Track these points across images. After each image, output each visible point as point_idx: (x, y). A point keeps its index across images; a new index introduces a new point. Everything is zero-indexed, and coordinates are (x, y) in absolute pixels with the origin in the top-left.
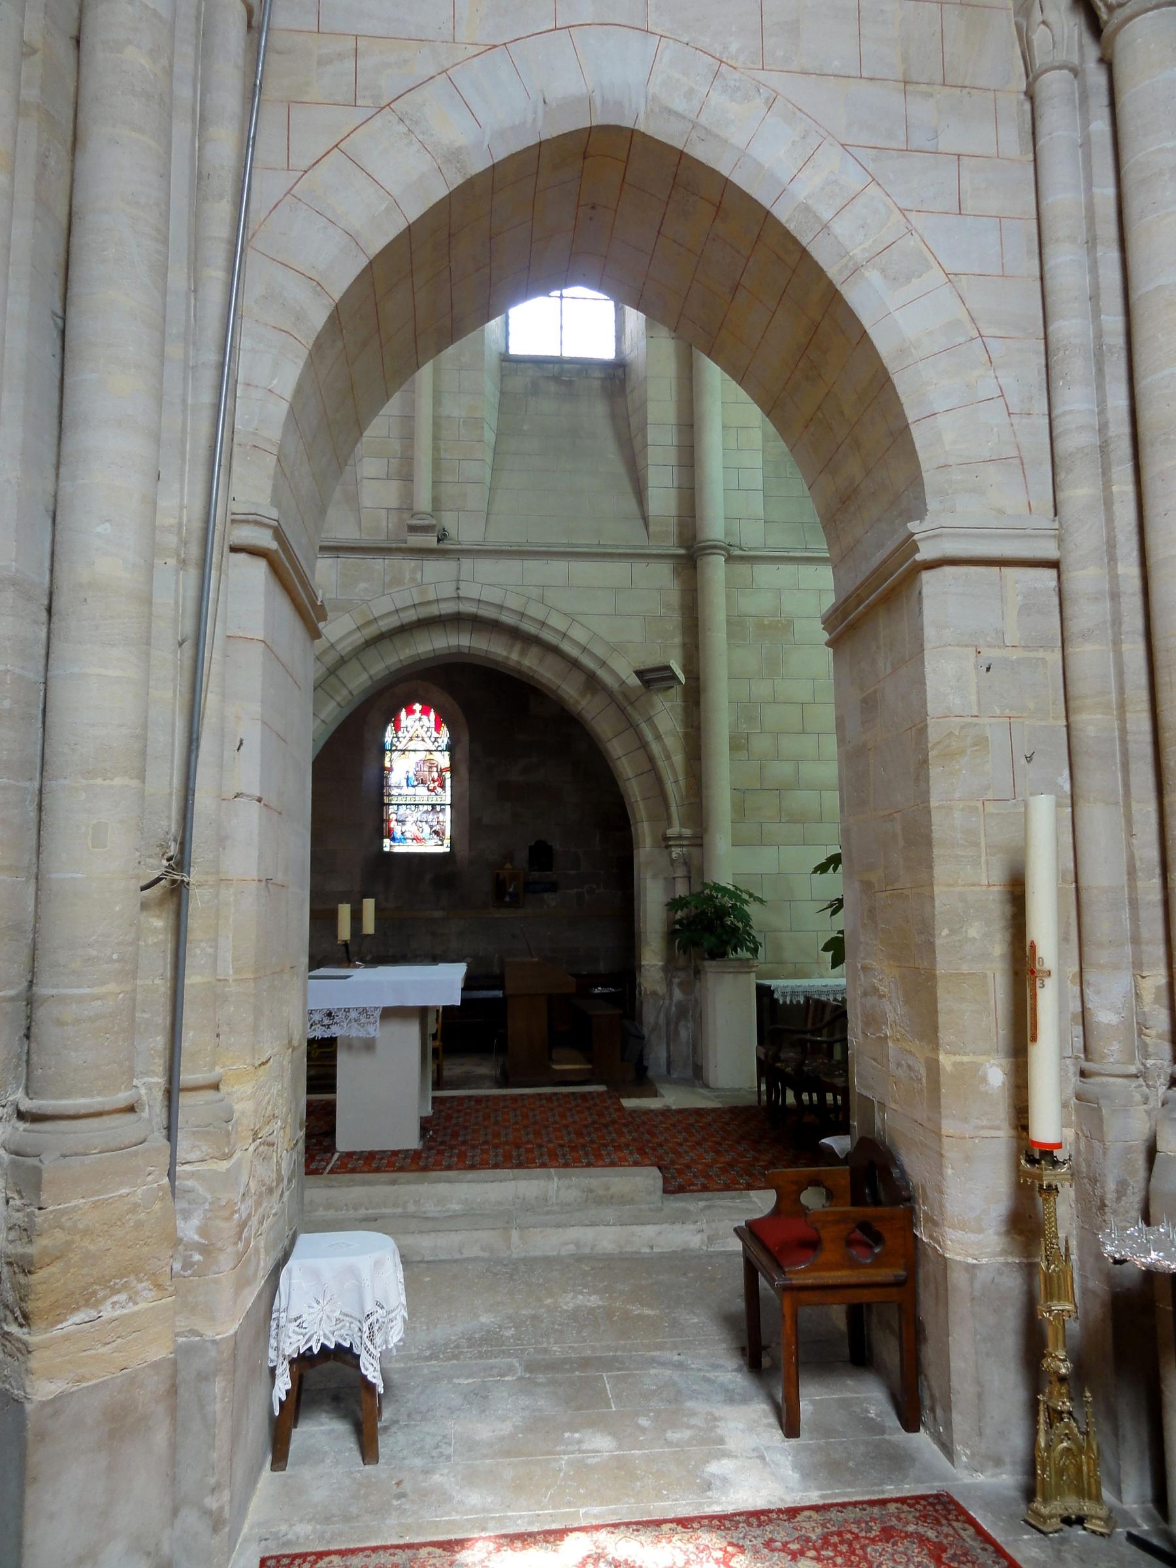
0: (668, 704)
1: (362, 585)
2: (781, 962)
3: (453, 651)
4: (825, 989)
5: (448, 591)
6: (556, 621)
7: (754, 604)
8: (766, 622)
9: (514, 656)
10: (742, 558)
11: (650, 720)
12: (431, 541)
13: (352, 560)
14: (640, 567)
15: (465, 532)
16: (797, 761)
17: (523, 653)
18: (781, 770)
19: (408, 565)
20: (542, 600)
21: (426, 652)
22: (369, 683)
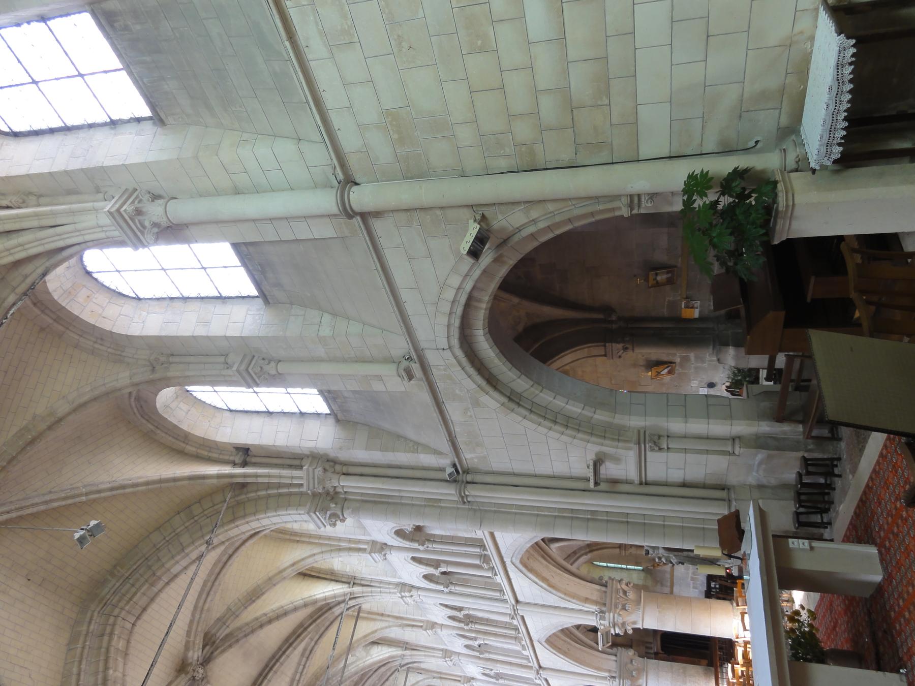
0: (500, 217)
1: (457, 391)
2: (782, 91)
3: (488, 335)
4: (832, 107)
5: (448, 354)
6: (449, 294)
7: (382, 150)
8: (396, 136)
9: (484, 306)
10: (343, 164)
11: (519, 230)
12: (416, 368)
13: (442, 396)
14: (384, 243)
15: (400, 346)
16: (536, 92)
17: (480, 301)
18: (549, 108)
19: (436, 373)
20: (436, 304)
21: (494, 351)
22: (523, 376)
